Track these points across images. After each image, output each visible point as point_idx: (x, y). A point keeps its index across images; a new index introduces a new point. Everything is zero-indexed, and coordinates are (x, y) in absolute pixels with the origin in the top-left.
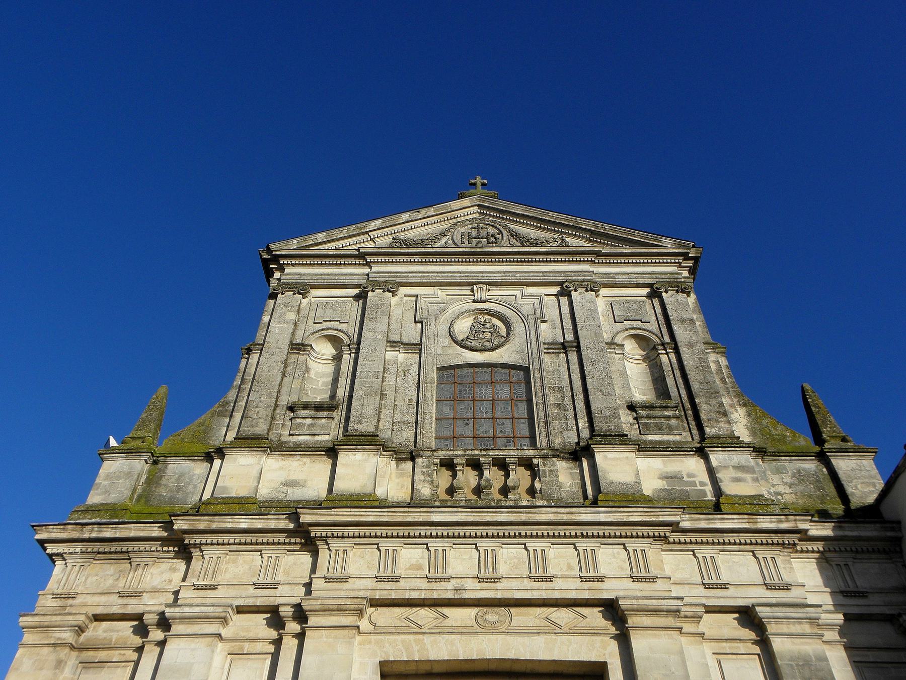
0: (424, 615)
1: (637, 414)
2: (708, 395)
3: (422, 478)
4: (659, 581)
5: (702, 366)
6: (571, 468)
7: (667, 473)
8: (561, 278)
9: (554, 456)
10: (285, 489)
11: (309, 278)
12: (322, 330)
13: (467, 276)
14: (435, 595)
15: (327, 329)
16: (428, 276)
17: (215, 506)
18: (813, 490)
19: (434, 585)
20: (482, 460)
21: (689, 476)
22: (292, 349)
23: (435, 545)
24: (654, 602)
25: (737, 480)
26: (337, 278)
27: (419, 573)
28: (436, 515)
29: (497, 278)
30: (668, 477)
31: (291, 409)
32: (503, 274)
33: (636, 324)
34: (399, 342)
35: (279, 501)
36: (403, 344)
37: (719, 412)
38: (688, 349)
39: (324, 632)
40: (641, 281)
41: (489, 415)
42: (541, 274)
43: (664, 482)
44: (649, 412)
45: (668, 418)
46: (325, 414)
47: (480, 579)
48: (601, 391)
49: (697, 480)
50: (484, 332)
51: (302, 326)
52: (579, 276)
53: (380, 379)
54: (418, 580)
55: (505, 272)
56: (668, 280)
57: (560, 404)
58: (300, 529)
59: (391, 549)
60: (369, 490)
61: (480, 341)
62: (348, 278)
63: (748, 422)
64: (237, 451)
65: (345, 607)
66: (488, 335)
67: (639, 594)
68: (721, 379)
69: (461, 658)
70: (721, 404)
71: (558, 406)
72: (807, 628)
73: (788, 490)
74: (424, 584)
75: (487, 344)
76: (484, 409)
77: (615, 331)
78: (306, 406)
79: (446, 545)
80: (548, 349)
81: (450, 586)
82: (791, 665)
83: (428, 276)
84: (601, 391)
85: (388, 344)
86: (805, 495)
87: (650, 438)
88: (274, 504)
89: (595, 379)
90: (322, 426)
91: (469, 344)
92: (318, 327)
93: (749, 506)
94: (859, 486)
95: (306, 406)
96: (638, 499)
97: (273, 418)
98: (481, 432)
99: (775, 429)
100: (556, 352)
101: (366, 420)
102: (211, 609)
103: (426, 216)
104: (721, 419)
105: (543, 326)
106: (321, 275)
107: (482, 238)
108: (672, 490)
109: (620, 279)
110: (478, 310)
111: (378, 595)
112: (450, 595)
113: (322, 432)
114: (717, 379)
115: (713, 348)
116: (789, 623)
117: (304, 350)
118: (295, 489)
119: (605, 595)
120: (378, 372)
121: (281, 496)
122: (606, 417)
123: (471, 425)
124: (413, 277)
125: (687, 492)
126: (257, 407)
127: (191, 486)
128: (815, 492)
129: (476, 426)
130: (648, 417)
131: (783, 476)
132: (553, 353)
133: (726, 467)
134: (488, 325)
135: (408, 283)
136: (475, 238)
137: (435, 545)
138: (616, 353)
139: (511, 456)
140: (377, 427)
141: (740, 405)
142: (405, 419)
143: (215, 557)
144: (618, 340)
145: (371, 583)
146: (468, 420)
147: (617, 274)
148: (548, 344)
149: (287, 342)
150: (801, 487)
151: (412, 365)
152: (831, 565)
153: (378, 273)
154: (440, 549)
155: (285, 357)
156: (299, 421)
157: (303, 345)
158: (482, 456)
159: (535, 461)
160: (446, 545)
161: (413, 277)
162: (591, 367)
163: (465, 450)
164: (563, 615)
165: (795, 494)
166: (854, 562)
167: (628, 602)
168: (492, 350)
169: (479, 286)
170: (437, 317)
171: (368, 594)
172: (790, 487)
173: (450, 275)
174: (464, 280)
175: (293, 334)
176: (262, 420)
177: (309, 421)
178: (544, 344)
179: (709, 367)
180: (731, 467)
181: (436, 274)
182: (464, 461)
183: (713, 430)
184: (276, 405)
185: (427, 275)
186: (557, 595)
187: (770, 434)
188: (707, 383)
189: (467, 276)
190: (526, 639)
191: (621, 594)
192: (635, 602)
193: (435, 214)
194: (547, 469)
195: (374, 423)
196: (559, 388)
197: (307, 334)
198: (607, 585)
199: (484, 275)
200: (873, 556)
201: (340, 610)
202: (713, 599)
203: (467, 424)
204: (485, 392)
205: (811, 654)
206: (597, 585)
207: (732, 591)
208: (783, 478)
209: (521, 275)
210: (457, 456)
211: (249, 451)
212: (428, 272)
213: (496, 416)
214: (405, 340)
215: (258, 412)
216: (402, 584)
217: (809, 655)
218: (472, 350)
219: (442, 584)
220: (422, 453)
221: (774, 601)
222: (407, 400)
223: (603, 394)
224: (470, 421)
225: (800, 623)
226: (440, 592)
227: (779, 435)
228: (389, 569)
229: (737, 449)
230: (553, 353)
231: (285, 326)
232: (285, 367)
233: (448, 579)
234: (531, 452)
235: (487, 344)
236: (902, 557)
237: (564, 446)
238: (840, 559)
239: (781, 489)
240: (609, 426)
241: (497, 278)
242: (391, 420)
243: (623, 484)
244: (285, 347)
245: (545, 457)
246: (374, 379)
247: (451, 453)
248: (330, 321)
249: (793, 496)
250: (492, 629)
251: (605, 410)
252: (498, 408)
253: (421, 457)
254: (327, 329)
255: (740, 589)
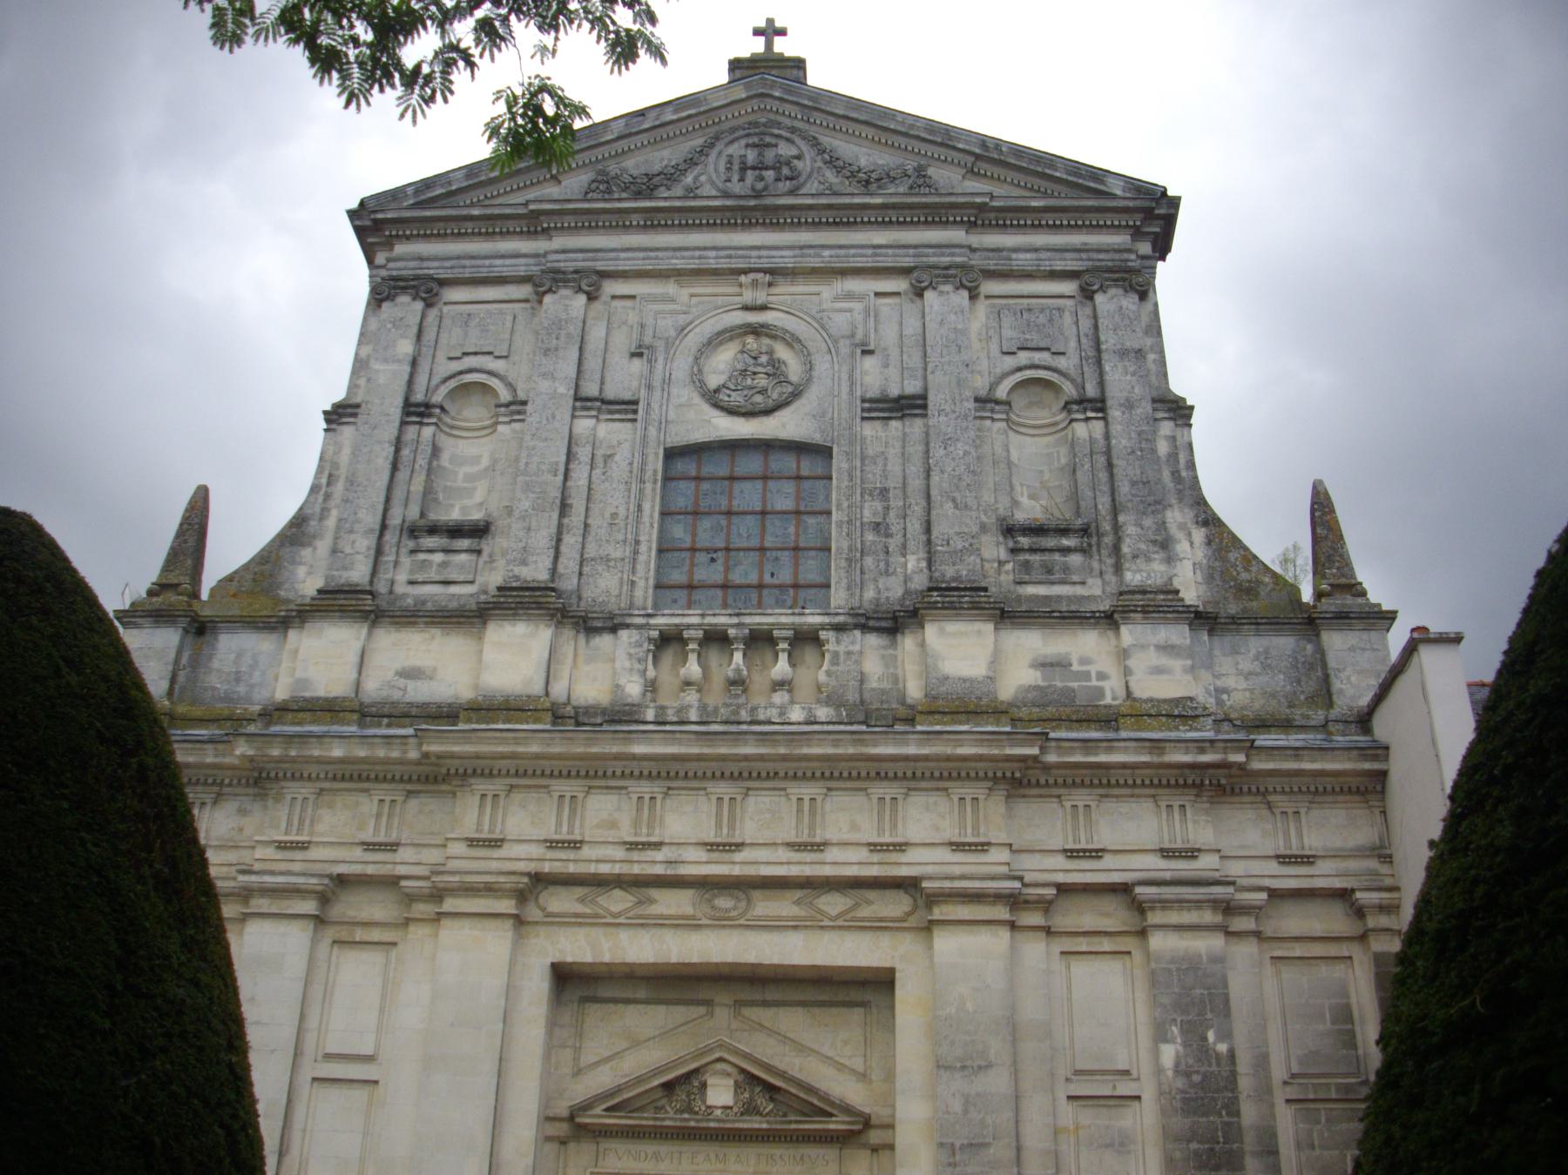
0: (618, 901)
1: (1016, 542)
2: (1141, 507)
3: (627, 664)
4: (993, 850)
5: (1141, 450)
6: (884, 648)
7: (1046, 656)
8: (907, 259)
9: (856, 626)
10: (402, 682)
11: (436, 264)
12: (461, 373)
13: (730, 257)
14: (636, 869)
15: (470, 371)
16: (657, 258)
17: (295, 714)
18: (1282, 683)
19: (635, 856)
20: (732, 632)
21: (1084, 661)
22: (408, 414)
23: (639, 789)
24: (977, 884)
25: (1158, 671)
26: (487, 262)
27: (611, 835)
28: (639, 744)
29: (786, 260)
30: (1046, 665)
31: (413, 531)
32: (797, 252)
33: (1038, 357)
34: (596, 399)
35: (394, 704)
36: (603, 401)
37: (1154, 542)
38: (1123, 413)
39: (467, 922)
40: (1059, 265)
41: (755, 542)
42: (870, 252)
43: (1038, 674)
44: (1035, 539)
45: (1066, 551)
46: (465, 543)
47: (712, 847)
48: (954, 500)
49: (1093, 669)
50: (755, 373)
51: (424, 366)
52: (943, 255)
53: (560, 477)
54: (611, 847)
55: (801, 248)
56: (1109, 264)
57: (878, 524)
58: (424, 761)
59: (568, 795)
60: (537, 688)
61: (745, 392)
62: (508, 262)
63: (1205, 556)
64: (322, 617)
65: (496, 886)
66: (762, 381)
67: (957, 870)
68: (1173, 474)
69: (674, 960)
70: (1162, 525)
71: (876, 527)
72: (1208, 917)
73: (1243, 684)
74: (620, 853)
75: (758, 399)
76: (744, 533)
77: (998, 371)
78: (433, 530)
79: (656, 789)
80: (869, 410)
81: (659, 856)
82: (1169, 970)
83: (657, 258)
84: (954, 500)
85: (578, 404)
86: (1265, 693)
87: (1031, 590)
88: (386, 710)
89: (946, 475)
90: (462, 567)
91: (726, 399)
92: (456, 366)
93: (1164, 719)
94: (1353, 679)
95: (433, 530)
96: (984, 709)
97: (379, 552)
98: (736, 577)
99: (1247, 570)
100: (883, 418)
101: (534, 558)
102: (301, 880)
103: (657, 123)
104: (1156, 556)
105: (869, 363)
106: (458, 258)
107: (767, 168)
108: (1048, 687)
109: (1023, 260)
110: (749, 325)
111: (547, 868)
112: (659, 870)
113: (461, 578)
114: (1166, 475)
115: (1169, 410)
116: (1182, 909)
117: (430, 415)
118: (419, 683)
119: (904, 872)
120: (557, 463)
121: (396, 695)
122: (955, 552)
123: (720, 561)
124: (629, 259)
125: (1073, 691)
126: (351, 532)
127: (257, 674)
128: (1284, 686)
129: (731, 563)
130: (1032, 550)
131: (1239, 658)
132: (878, 418)
133: (1143, 647)
134: (764, 359)
135: (617, 272)
136: (754, 168)
137: (639, 789)
138: (993, 420)
139: (782, 627)
140: (554, 571)
141: (1197, 523)
142: (602, 553)
143: (300, 797)
144: (1002, 392)
145: (536, 851)
146: (716, 551)
147: (1016, 250)
148: (871, 401)
149: (399, 401)
150: (1264, 679)
151: (620, 443)
152: (1273, 813)
153: (564, 251)
154: (647, 797)
155: (395, 432)
156: (422, 556)
157: (427, 406)
158: (732, 626)
159: (823, 635)
160: (656, 789)
161: (629, 259)
162: (942, 452)
163: (703, 615)
164: (834, 904)
165: (1252, 691)
166: (1309, 808)
167: (936, 884)
168: (768, 412)
169: (752, 276)
170: (669, 344)
171: (532, 867)
172: (1246, 679)
173: (697, 253)
174: (724, 264)
175: (410, 383)
176: (360, 557)
177: (438, 558)
178: (863, 401)
179: (1153, 451)
180: (1152, 648)
181: (670, 254)
182: (700, 634)
183: (1138, 577)
184: (384, 527)
185: (652, 254)
186: (828, 871)
187: (1235, 579)
188: (1144, 483)
189: (730, 257)
190: (775, 937)
191: (929, 870)
192: (947, 884)
193: (675, 117)
194: (841, 649)
195: (548, 563)
196: (881, 492)
197: (435, 381)
198: (912, 855)
199: (764, 253)
200: (1341, 798)
201: (489, 890)
202: (1075, 874)
203: (713, 560)
204: (748, 496)
205: (1203, 952)
206: (894, 857)
207: (1108, 861)
208: (1237, 663)
209: (833, 252)
210: (689, 626)
211: (342, 617)
212: (657, 249)
213: (767, 544)
214: (610, 393)
215: (354, 542)
216: (586, 852)
217: (1200, 956)
218: (732, 411)
219: (650, 853)
220: (629, 620)
221: (1168, 875)
222: (607, 515)
223: (956, 507)
224: (720, 554)
225: (1199, 908)
226: (644, 866)
227: (1249, 581)
228: (565, 828)
229: (1169, 615)
230: (878, 418)
231: (395, 367)
232: (397, 450)
233: (658, 845)
234: (818, 620)
235: (758, 399)
236: (1383, 800)
237: (877, 605)
238: (1288, 804)
239: (1230, 682)
240: (958, 571)
241: (786, 260)
242: (578, 557)
243: (965, 681)
244: (396, 412)
245: (839, 628)
246: (550, 477)
247: (677, 620)
248: (476, 353)
249: (1247, 694)
250: (722, 922)
251: (956, 538)
252: (770, 529)
253: (628, 626)
254: (470, 371)
255: (1119, 857)
